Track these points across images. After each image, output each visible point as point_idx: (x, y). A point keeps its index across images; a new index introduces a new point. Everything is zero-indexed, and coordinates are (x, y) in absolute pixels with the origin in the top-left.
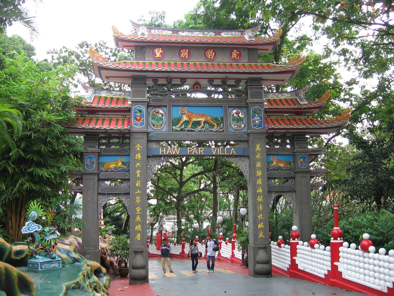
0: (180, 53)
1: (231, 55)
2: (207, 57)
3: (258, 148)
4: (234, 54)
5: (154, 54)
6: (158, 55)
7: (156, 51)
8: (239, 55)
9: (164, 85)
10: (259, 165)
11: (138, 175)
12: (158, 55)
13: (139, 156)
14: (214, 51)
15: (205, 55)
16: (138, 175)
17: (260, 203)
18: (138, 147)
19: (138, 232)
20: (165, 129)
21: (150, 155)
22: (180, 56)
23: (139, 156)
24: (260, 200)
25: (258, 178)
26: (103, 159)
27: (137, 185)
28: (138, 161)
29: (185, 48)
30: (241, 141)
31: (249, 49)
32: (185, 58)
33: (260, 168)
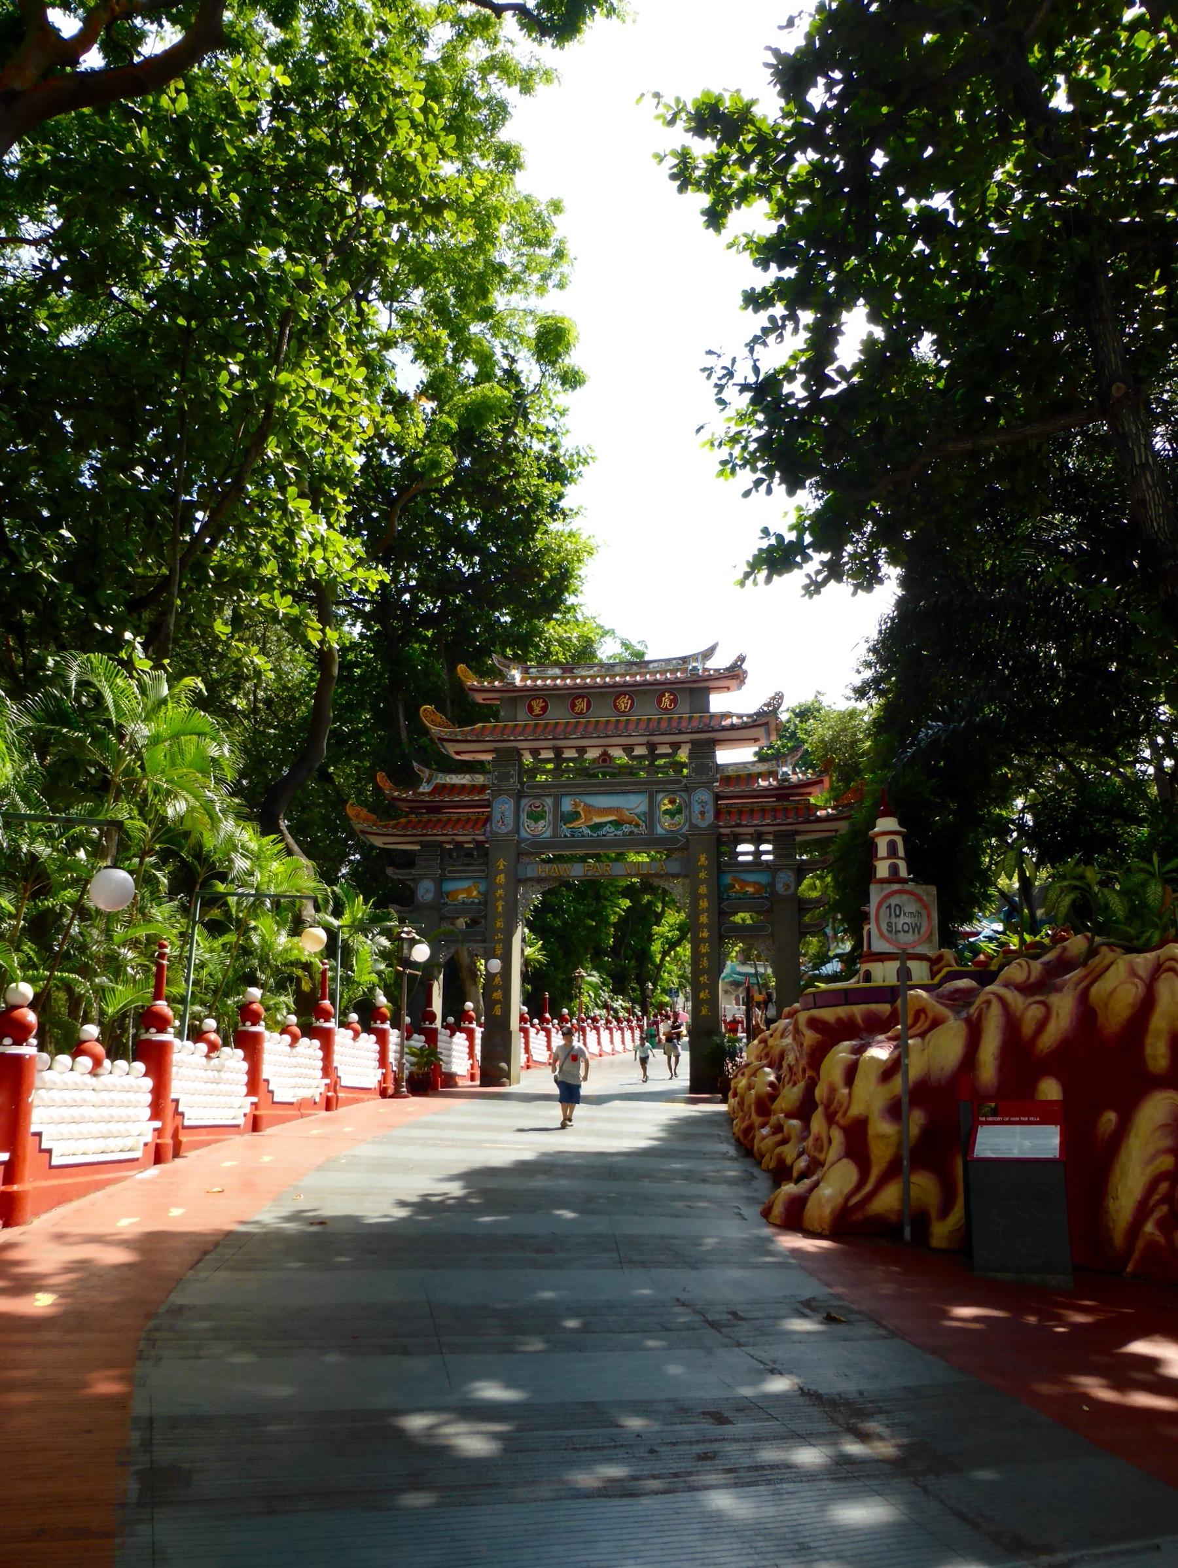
0: (573, 706)
1: (660, 702)
2: (618, 710)
3: (703, 860)
4: (666, 701)
5: (531, 709)
6: (537, 711)
7: (534, 703)
8: (674, 701)
9: (548, 761)
10: (703, 890)
11: (500, 909)
12: (537, 711)
13: (501, 878)
14: (631, 698)
15: (616, 706)
16: (500, 909)
17: (704, 955)
18: (502, 864)
19: (497, 1002)
20: (548, 833)
21: (522, 876)
22: (573, 709)
23: (501, 878)
24: (704, 951)
25: (703, 911)
26: (449, 886)
27: (498, 925)
28: (501, 886)
29: (582, 696)
30: (676, 849)
31: (691, 689)
32: (581, 713)
33: (705, 896)
